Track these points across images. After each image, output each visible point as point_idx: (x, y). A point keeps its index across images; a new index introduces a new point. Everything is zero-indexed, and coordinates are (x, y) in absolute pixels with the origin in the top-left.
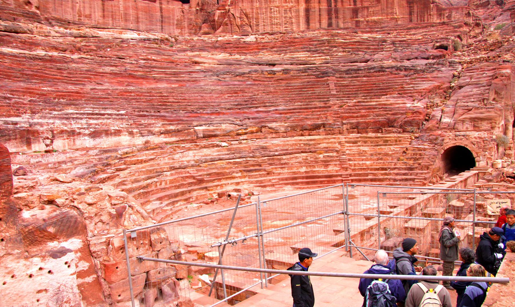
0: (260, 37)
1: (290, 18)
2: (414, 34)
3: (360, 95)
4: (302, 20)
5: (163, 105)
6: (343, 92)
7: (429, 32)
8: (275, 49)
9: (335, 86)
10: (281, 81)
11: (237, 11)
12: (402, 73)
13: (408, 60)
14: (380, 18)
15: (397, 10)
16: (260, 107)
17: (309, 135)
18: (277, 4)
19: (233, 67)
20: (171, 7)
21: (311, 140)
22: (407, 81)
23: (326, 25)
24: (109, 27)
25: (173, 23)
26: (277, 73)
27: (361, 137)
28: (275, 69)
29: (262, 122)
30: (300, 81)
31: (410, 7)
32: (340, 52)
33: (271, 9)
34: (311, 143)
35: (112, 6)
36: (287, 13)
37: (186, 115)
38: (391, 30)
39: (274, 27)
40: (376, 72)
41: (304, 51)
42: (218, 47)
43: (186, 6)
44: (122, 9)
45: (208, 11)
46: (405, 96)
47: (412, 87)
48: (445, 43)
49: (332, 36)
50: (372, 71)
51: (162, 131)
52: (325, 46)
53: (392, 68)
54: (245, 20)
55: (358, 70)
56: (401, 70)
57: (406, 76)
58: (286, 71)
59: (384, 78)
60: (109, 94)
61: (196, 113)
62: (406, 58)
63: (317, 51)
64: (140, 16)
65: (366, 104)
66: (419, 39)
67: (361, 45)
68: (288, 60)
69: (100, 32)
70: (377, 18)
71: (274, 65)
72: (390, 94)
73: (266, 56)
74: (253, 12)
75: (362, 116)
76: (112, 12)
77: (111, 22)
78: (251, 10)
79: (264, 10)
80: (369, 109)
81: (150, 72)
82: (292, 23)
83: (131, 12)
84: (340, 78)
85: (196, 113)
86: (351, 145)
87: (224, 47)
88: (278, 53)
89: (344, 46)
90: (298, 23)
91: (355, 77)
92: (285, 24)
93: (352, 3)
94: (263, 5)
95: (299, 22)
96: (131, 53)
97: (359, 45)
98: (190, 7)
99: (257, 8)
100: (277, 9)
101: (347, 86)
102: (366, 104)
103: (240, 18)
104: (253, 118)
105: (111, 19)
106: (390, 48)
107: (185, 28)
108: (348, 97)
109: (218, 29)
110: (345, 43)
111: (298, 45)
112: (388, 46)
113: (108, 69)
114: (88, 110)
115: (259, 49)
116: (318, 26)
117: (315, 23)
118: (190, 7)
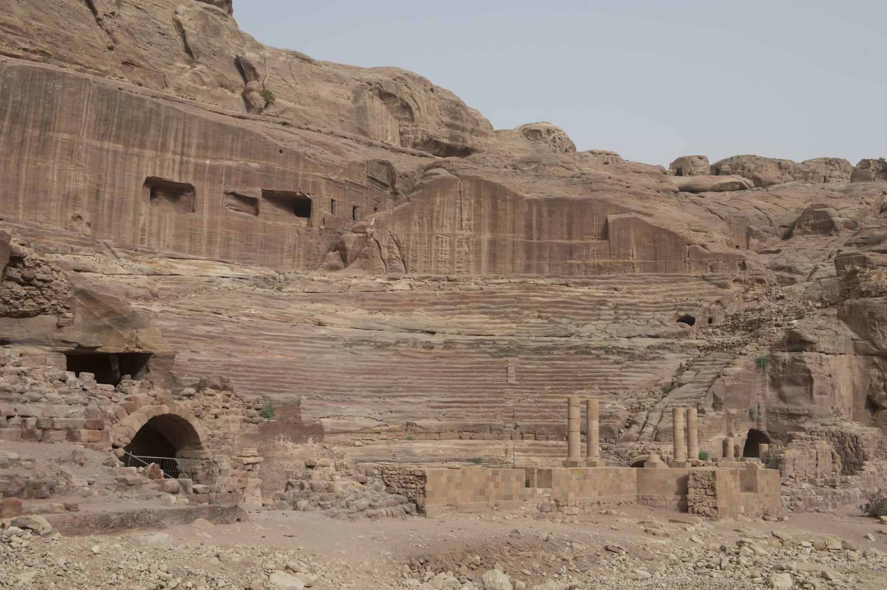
0: (418, 283)
1: (466, 253)
2: (654, 293)
3: (547, 388)
4: (484, 258)
6: (525, 381)
7: (676, 290)
9: (516, 371)
10: (440, 360)
11: (384, 237)
12: (613, 358)
13: (629, 338)
14: (607, 261)
15: (634, 250)
16: (407, 396)
17: (471, 439)
18: (447, 230)
19: (373, 334)
20: (280, 223)
21: (469, 445)
22: (616, 370)
23: (523, 268)
25: (282, 249)
27: (534, 444)
28: (433, 339)
29: (410, 417)
30: (468, 360)
31: (655, 247)
32: (534, 317)
33: (437, 238)
34: (469, 448)
35: (191, 219)
36: (461, 246)
37: (309, 402)
38: (620, 283)
39: (440, 265)
40: (577, 353)
42: (352, 297)
43: (303, 222)
44: (205, 225)
45: (338, 230)
46: (606, 392)
47: (620, 380)
48: (691, 314)
49: (529, 289)
50: (572, 352)
52: (513, 307)
53: (601, 348)
54: (396, 251)
56: (614, 354)
57: (617, 363)
58: (448, 345)
59: (587, 363)
61: (322, 399)
62: (625, 335)
63: (502, 313)
64: (233, 236)
65: (553, 400)
66: (658, 303)
67: (567, 308)
68: (455, 327)
69: (180, 266)
71: (433, 333)
72: (588, 388)
73: (422, 318)
74: (409, 240)
75: (544, 417)
76: (191, 229)
77: (187, 244)
79: (426, 238)
80: (555, 407)
81: (256, 335)
82: (469, 262)
84: (526, 359)
85: (322, 399)
86: (521, 454)
87: (361, 298)
88: (442, 313)
89: (540, 309)
90: (478, 263)
91: (546, 360)
92: (458, 262)
93: (565, 236)
94: (426, 230)
95: (480, 262)
96: (225, 302)
97: (563, 308)
98: (310, 225)
100: (448, 238)
101: (534, 372)
102: (553, 400)
103: (389, 248)
104: (396, 412)
105: (188, 239)
106: (610, 315)
107: (299, 257)
108: (531, 389)
109: (351, 262)
111: (473, 302)
112: (607, 313)
113: (202, 329)
115: (414, 305)
116: (509, 266)
118: (310, 225)
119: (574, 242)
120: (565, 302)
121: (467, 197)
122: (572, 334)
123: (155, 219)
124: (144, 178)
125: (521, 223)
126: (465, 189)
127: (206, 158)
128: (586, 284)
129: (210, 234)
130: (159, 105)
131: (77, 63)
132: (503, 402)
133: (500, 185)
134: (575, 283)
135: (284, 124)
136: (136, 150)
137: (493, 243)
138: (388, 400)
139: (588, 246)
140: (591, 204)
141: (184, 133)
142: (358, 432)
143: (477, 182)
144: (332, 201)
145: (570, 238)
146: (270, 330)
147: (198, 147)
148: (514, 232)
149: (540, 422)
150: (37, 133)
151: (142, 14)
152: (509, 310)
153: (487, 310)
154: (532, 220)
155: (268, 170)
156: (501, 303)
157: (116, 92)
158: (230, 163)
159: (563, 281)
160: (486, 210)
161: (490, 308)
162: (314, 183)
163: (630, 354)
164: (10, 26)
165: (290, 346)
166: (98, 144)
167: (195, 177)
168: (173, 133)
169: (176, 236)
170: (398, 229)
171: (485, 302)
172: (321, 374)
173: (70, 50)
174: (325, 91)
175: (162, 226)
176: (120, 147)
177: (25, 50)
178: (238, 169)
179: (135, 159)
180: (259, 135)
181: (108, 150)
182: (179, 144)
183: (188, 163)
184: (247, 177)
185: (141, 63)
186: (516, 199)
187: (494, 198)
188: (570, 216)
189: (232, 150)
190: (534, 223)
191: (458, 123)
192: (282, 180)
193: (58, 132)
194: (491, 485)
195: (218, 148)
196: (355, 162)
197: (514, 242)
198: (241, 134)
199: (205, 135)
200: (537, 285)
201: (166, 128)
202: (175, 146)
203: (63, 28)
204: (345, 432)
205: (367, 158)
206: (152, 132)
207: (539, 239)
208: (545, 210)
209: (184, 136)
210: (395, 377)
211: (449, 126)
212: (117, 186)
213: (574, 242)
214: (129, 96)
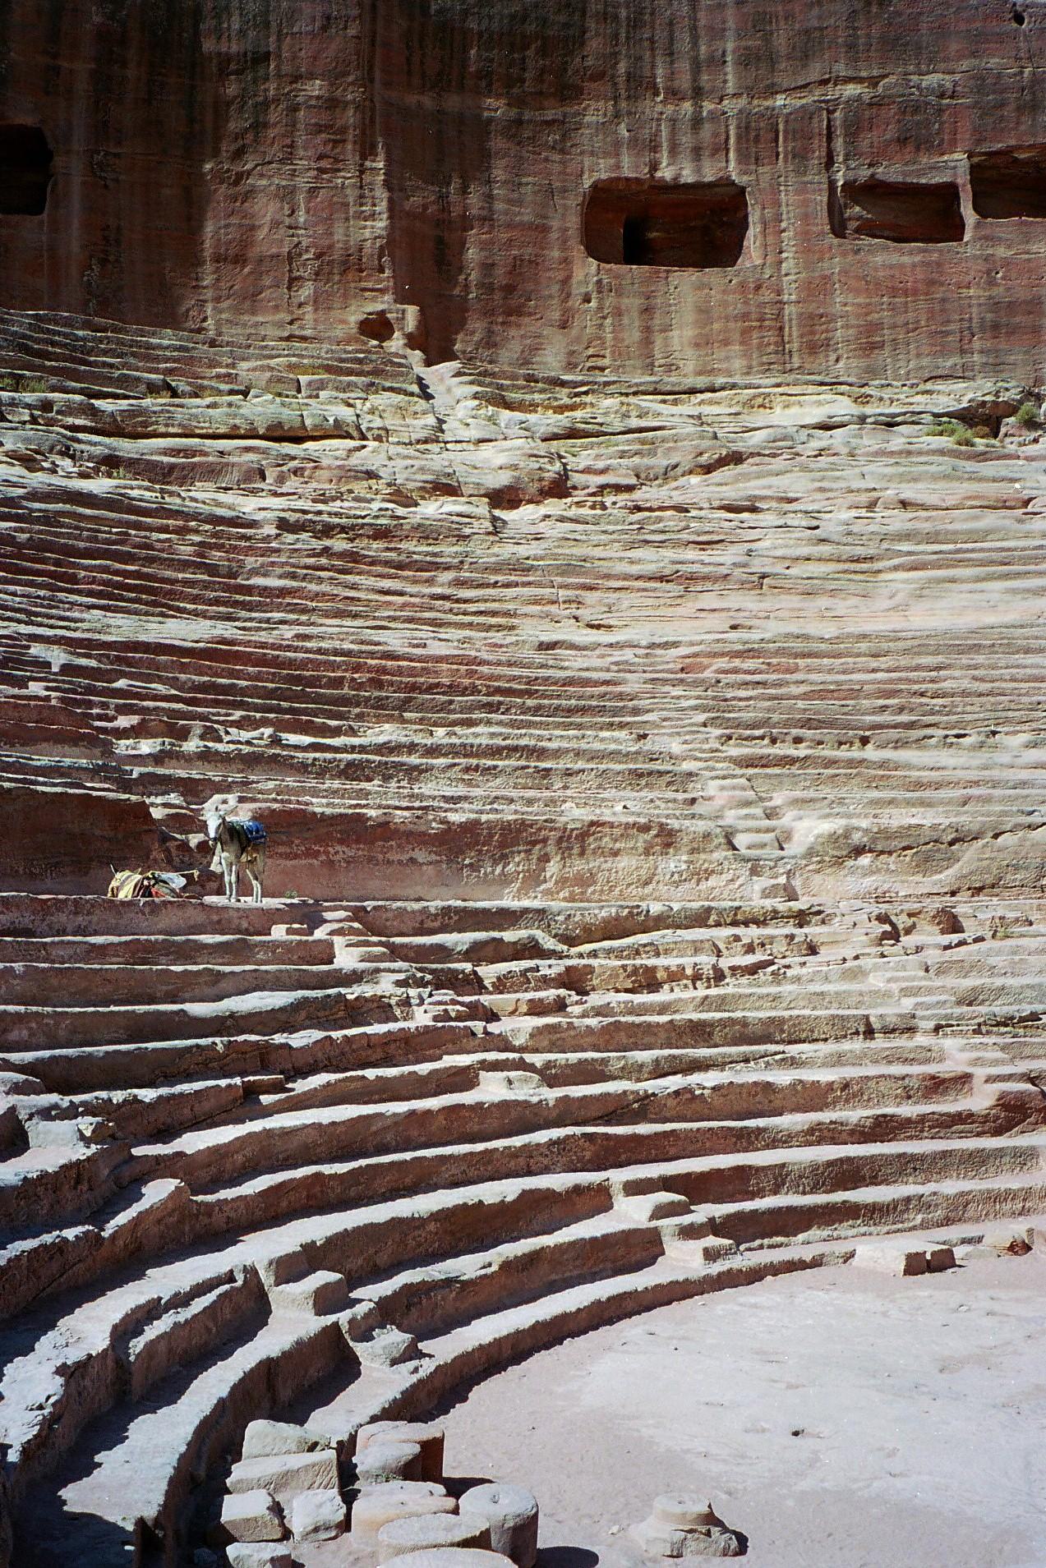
5: (901, 710)
24: (720, 381)
51: (857, 838)
60: (626, 667)
83: (842, 302)
96: (795, 483)
114: (480, 735)
123: (632, 303)
124: (587, 183)
127: (772, 91)
129: (811, 320)
155: (981, 82)
166: (428, 101)
167: (743, 158)
168: (661, 35)
169: (703, 343)
175: (657, 322)
178: (877, 103)
182: (684, 66)
183: (714, 117)
189: (851, 47)
193: (296, 78)
201: (635, 23)
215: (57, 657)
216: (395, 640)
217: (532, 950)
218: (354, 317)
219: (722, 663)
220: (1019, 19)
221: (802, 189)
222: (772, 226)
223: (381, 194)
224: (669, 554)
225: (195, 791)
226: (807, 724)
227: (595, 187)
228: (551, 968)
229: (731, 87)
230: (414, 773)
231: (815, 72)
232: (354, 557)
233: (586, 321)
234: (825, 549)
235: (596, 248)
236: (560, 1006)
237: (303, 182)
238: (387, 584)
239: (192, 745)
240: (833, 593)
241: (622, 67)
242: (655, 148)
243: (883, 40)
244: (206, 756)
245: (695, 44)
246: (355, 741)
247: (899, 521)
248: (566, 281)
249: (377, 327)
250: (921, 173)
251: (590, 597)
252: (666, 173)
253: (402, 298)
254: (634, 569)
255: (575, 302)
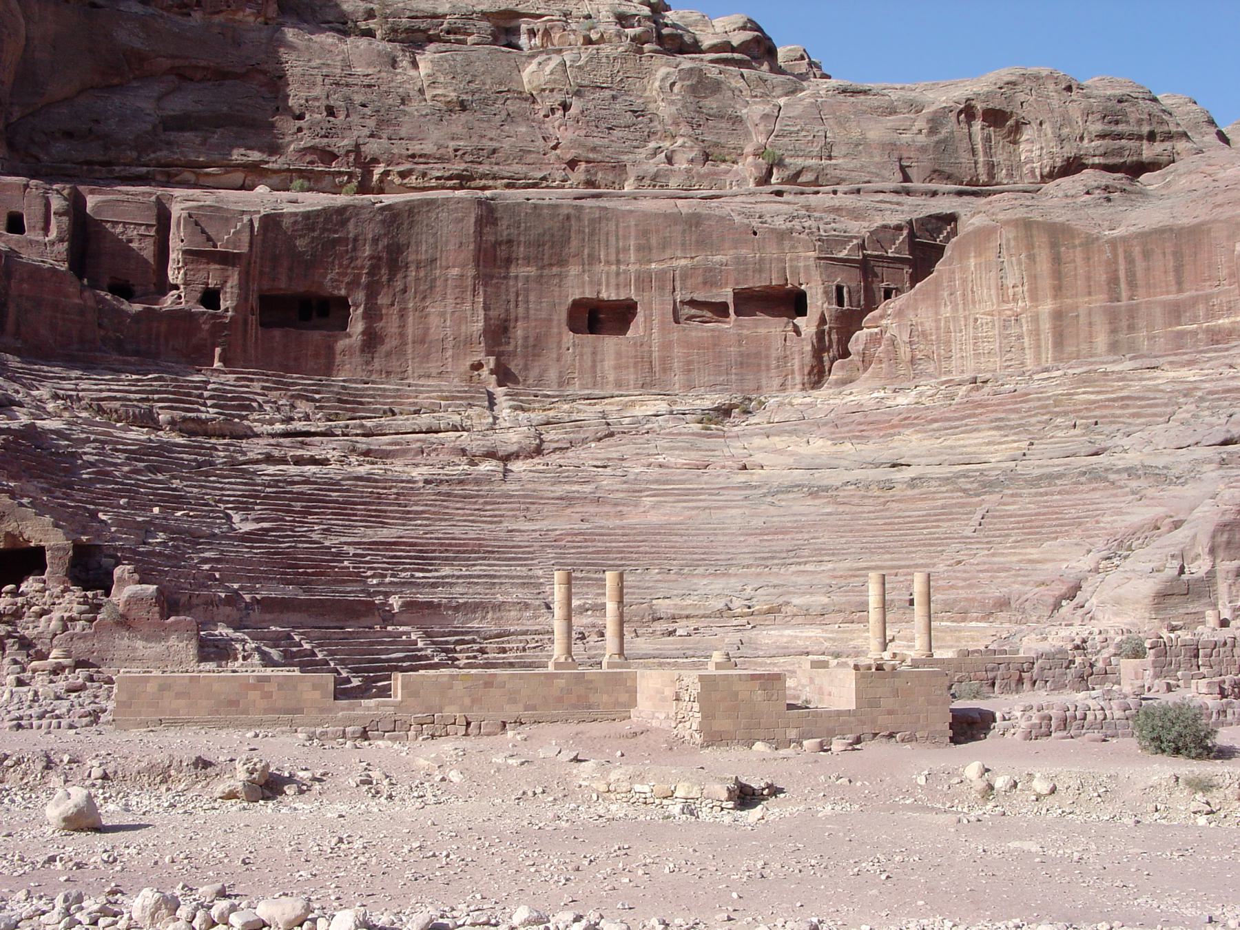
5: (622, 559)
8: (935, 425)
12: (1134, 484)
16: (806, 563)
19: (817, 474)
20: (762, 331)
26: (899, 486)
33: (976, 320)
37: (659, 577)
41: (990, 429)
50: (1083, 479)
55: (1060, 476)
57: (1133, 493)
58: (913, 483)
59: (1097, 494)
62: (1176, 444)
65: (1002, 559)
70: (1232, 319)
73: (910, 443)
74: (938, 328)
77: (632, 377)
78: (933, 324)
82: (1023, 349)
83: (677, 351)
84: (1012, 495)
88: (937, 435)
91: (1041, 494)
93: (1174, 288)
94: (961, 311)
95: (1039, 347)
97: (1121, 407)
99: (947, 320)
104: (775, 586)
107: (793, 372)
110: (1094, 402)
113: (560, 490)
114: (477, 570)
116: (1084, 347)
117: (1078, 346)
119: (1187, 294)
120: (1128, 398)
121: (1013, 251)
122: (1105, 450)
123: (588, 350)
124: (570, 300)
125: (1101, 276)
126: (1008, 240)
127: (650, 262)
128: (1190, 363)
129: (663, 360)
130: (581, 208)
131: (503, 178)
132: (934, 565)
133: (1063, 224)
134: (1171, 363)
135: (779, 193)
136: (555, 270)
137: (1058, 315)
138: (775, 570)
139: (1207, 298)
140: (1209, 230)
141: (617, 236)
142: (703, 616)
143: (1027, 225)
144: (839, 289)
145: (1180, 290)
146: (665, 483)
147: (639, 248)
148: (1090, 294)
149: (963, 594)
150: (422, 274)
151: (608, 93)
152: (1033, 420)
153: (1002, 424)
154: (1116, 270)
156: (1029, 410)
157: (519, 204)
158: (683, 262)
159: (1154, 362)
160: (1044, 265)
161: (1009, 420)
162: (807, 268)
163: (1161, 477)
164: (420, 156)
165: (685, 501)
167: (637, 289)
168: (603, 238)
169: (618, 367)
170: (924, 317)
171: (1005, 411)
172: (701, 538)
173: (497, 164)
174: (877, 131)
175: (599, 357)
176: (532, 271)
177: (438, 178)
178: (694, 268)
179: (556, 281)
180: (722, 218)
181: (516, 277)
182: (613, 250)
183: (625, 272)
184: (711, 277)
185: (591, 156)
186: (1090, 242)
187: (1054, 245)
188: (1178, 255)
189: (683, 245)
190: (1122, 274)
191: (1121, 128)
192: (760, 271)
194: (253, 695)
195: (664, 246)
196: (885, 227)
197: (1090, 310)
198: (694, 221)
199: (645, 233)
200: (1105, 373)
201: (592, 234)
202: (607, 255)
203: (491, 139)
204: (687, 617)
205: (915, 216)
206: (574, 243)
207: (1131, 298)
208: (1137, 250)
209: (617, 240)
210: (806, 536)
211: (1102, 136)
212: (532, 317)
213: (1187, 294)
214: (535, 206)
215: (351, 550)
216: (457, 532)
217: (474, 641)
218: (468, 363)
219: (569, 538)
220: (755, 233)
221: (662, 302)
222: (649, 319)
223: (482, 313)
224: (567, 487)
225: (387, 595)
226: (588, 564)
227: (574, 301)
228: (476, 647)
229: (632, 259)
230: (451, 585)
231: (668, 254)
232: (448, 494)
233: (568, 357)
234: (625, 486)
235: (574, 329)
236: (475, 657)
237: (449, 309)
238: (459, 505)
239: (387, 580)
240: (624, 505)
241: (586, 252)
242: (600, 285)
243: (697, 242)
244: (391, 583)
245: (617, 240)
246: (436, 574)
247: (655, 472)
248: (560, 342)
249: (478, 366)
250: (713, 297)
251: (533, 507)
252: (604, 295)
253: (489, 354)
254: (552, 495)
255: (563, 350)
